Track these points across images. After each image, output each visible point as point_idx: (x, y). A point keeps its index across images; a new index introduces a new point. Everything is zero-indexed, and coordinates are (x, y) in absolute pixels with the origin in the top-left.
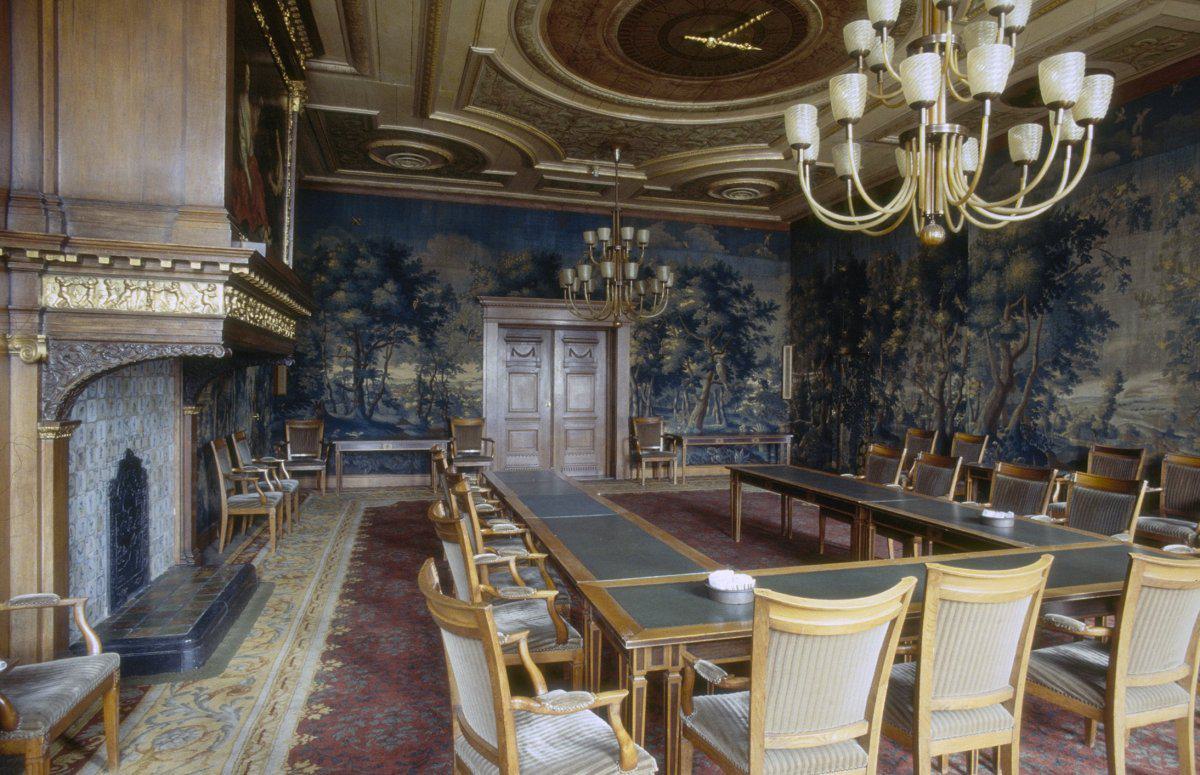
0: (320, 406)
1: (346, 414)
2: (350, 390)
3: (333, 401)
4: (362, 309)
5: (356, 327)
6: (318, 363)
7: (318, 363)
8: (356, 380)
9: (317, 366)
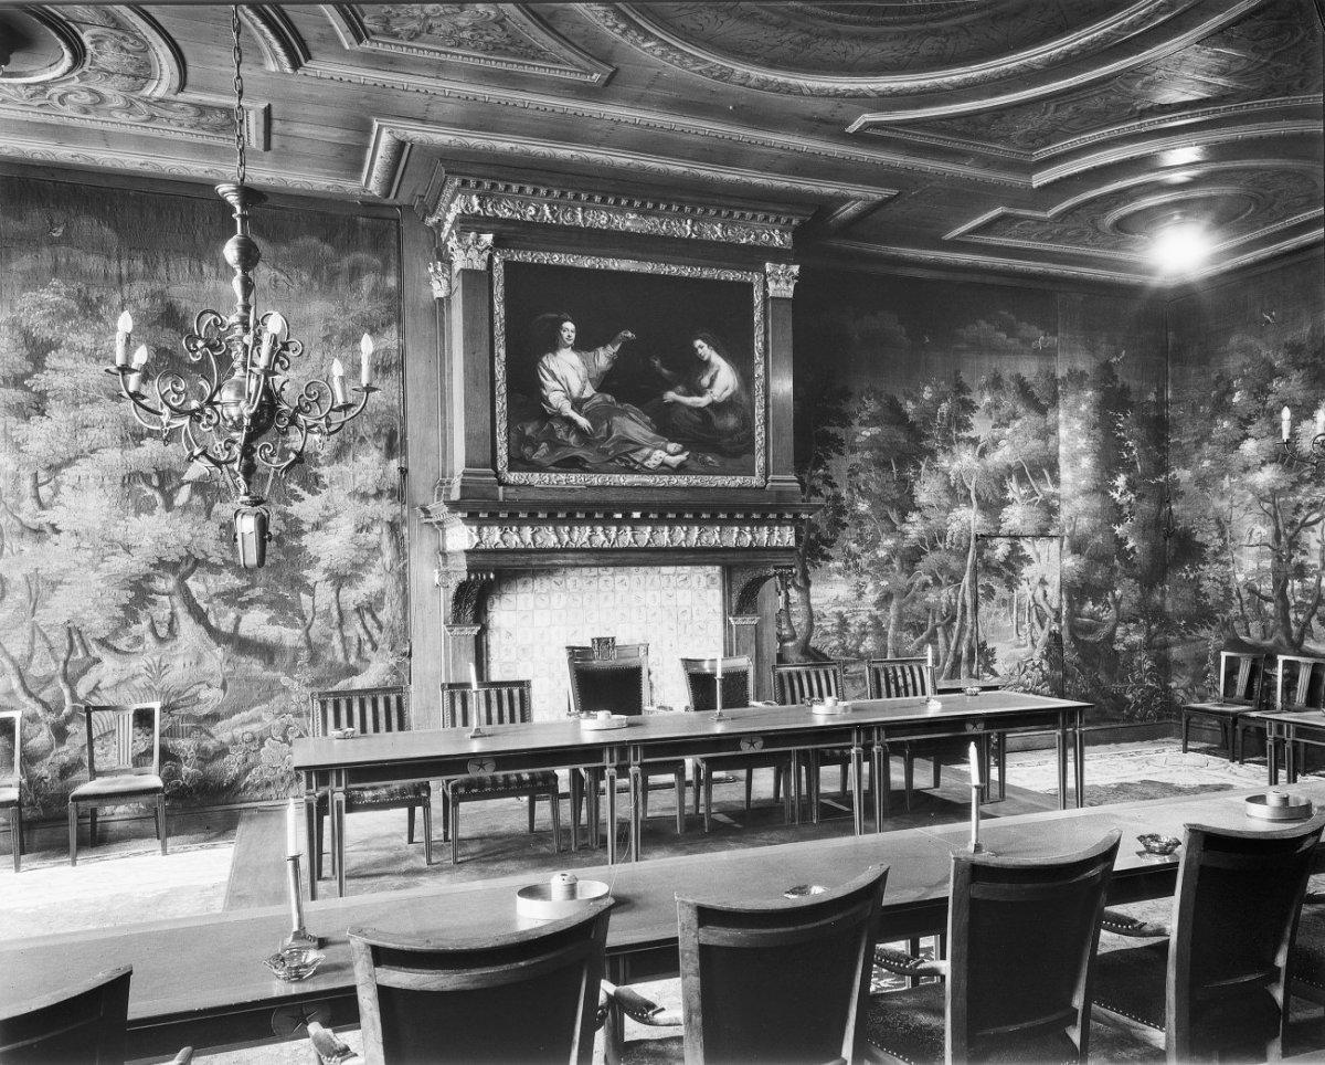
0: (1227, 625)
1: (1264, 638)
2: (1267, 599)
3: (1244, 617)
4: (1282, 463)
5: (1275, 493)
6: (1223, 558)
7: (1223, 558)
8: (1276, 582)
9: (1221, 562)
